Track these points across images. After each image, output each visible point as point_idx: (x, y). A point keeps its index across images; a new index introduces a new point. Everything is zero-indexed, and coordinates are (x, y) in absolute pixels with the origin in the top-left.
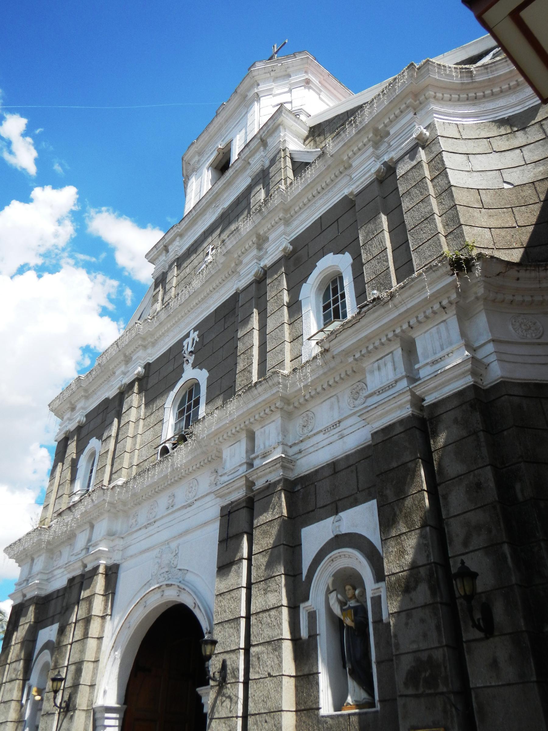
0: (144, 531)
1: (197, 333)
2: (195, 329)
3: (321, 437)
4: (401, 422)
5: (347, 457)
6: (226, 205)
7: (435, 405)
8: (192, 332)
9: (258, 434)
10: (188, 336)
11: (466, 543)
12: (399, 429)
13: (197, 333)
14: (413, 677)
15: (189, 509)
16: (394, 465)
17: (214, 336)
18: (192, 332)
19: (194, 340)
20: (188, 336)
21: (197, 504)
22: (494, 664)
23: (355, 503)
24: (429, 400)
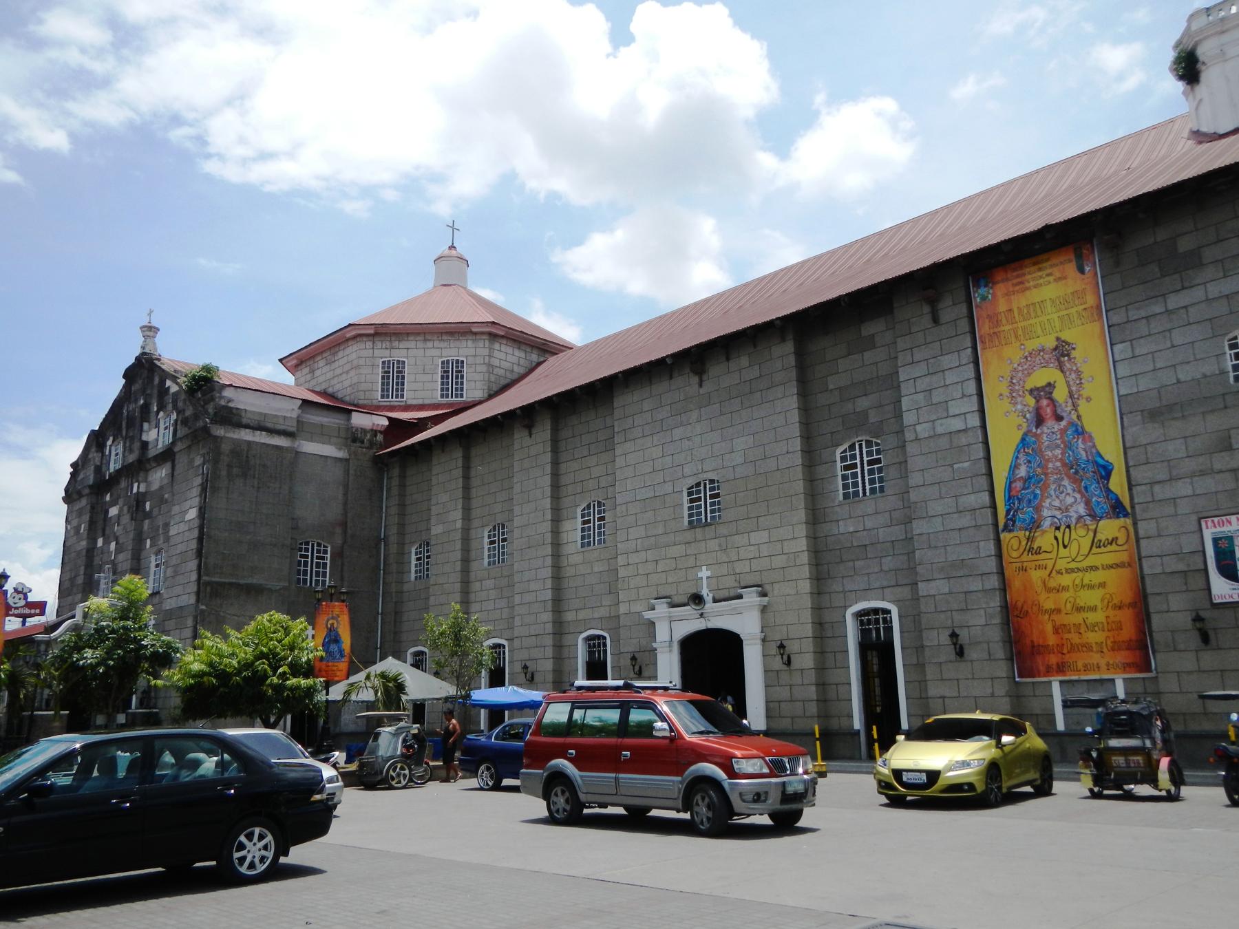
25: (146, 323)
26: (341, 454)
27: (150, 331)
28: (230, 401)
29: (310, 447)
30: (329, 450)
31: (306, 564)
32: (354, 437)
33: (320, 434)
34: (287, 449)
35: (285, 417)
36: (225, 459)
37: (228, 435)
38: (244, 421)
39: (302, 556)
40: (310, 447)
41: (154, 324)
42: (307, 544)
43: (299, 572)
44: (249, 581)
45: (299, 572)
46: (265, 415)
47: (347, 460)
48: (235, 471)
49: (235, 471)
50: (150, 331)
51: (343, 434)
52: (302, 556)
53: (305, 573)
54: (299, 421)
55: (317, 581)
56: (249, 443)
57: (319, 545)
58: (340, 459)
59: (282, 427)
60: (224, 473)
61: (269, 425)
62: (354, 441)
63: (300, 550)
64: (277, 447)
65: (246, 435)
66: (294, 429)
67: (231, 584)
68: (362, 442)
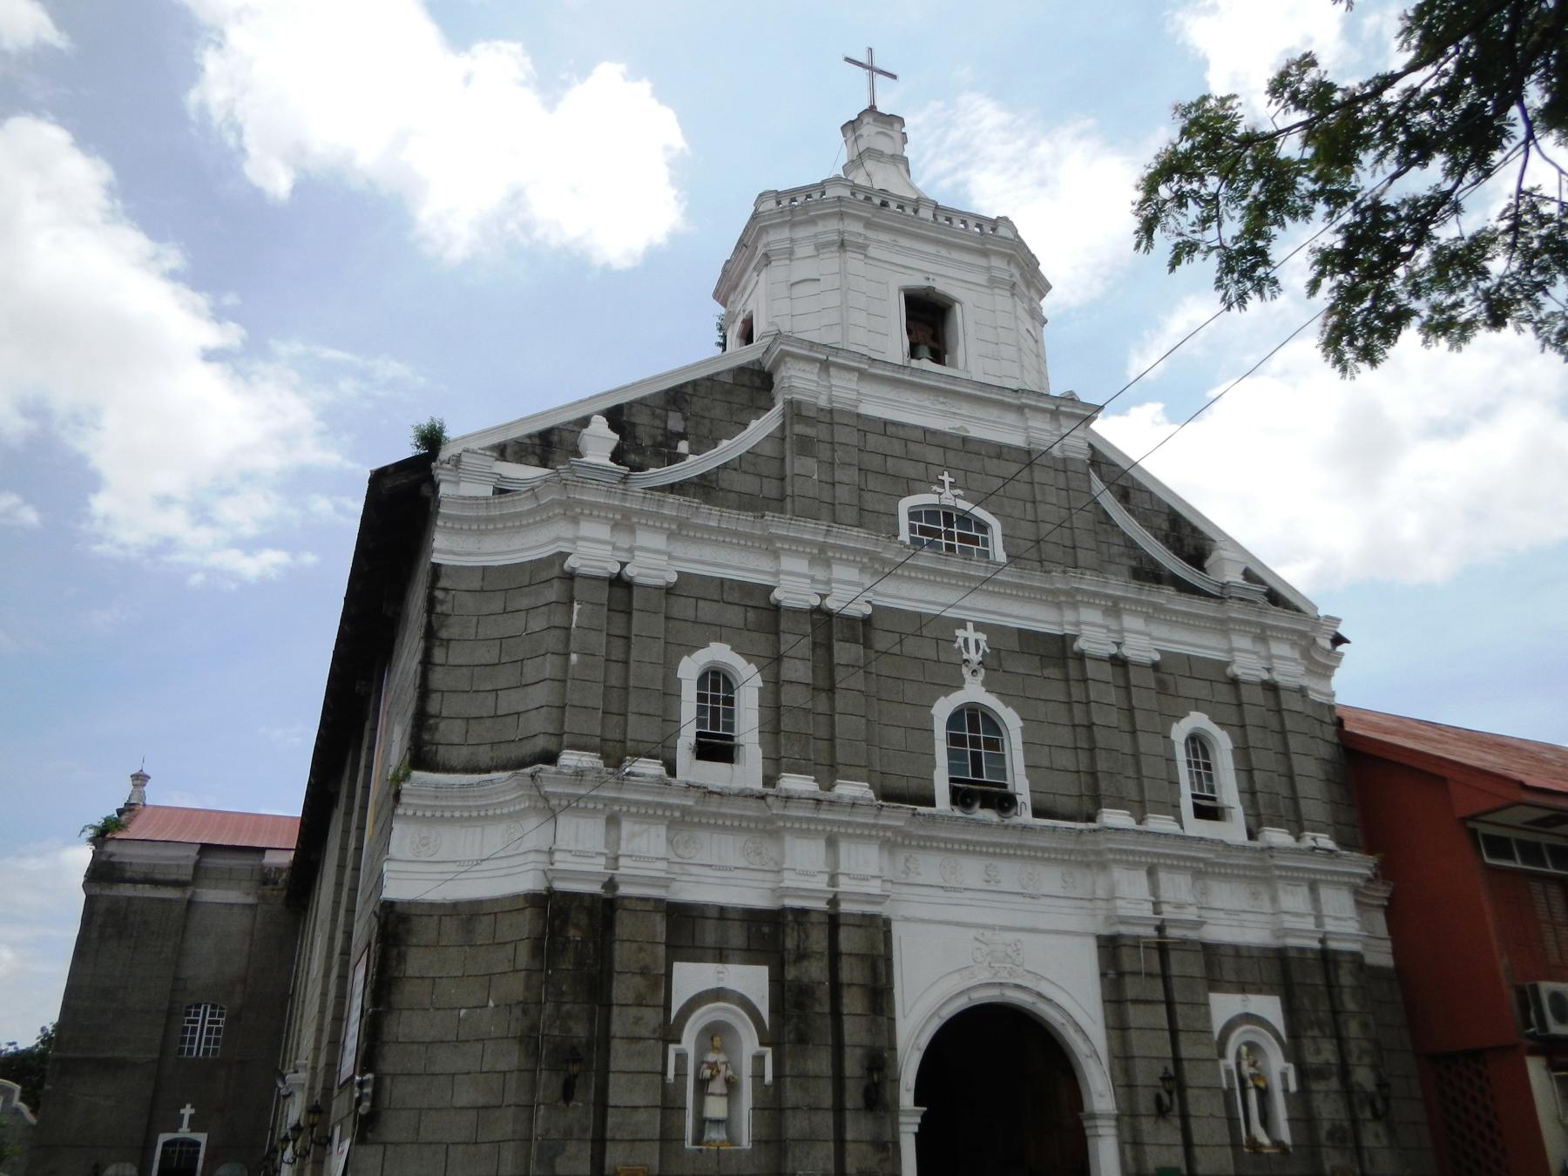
0: (941, 892)
1: (984, 637)
2: (979, 627)
3: (1221, 915)
4: (1312, 950)
5: (1249, 948)
6: (976, 432)
7: (1336, 952)
8: (970, 626)
9: (1163, 876)
10: (962, 624)
11: (1360, 1058)
12: (1310, 955)
13: (984, 637)
14: (1331, 1135)
15: (1028, 900)
16: (1308, 981)
17: (1022, 671)
18: (970, 626)
19: (977, 642)
20: (962, 624)
21: (1043, 900)
22: (1377, 1136)
23: (1260, 992)
24: (1333, 945)
25: (136, 771)
26: (251, 900)
27: (140, 779)
28: (111, 855)
29: (210, 895)
30: (234, 896)
31: (194, 1030)
32: (266, 878)
33: (228, 878)
34: (176, 901)
37: (107, 892)
38: (128, 874)
40: (210, 895)
41: (146, 772)
42: (198, 1006)
44: (109, 1054)
47: (251, 906)
50: (140, 779)
53: (192, 1041)
54: (197, 867)
55: (206, 1051)
56: (129, 899)
57: (214, 1007)
58: (244, 905)
59: (173, 877)
60: (95, 935)
61: (158, 876)
63: (188, 1014)
64: (163, 900)
65: (126, 891)
66: (189, 878)
68: (276, 883)
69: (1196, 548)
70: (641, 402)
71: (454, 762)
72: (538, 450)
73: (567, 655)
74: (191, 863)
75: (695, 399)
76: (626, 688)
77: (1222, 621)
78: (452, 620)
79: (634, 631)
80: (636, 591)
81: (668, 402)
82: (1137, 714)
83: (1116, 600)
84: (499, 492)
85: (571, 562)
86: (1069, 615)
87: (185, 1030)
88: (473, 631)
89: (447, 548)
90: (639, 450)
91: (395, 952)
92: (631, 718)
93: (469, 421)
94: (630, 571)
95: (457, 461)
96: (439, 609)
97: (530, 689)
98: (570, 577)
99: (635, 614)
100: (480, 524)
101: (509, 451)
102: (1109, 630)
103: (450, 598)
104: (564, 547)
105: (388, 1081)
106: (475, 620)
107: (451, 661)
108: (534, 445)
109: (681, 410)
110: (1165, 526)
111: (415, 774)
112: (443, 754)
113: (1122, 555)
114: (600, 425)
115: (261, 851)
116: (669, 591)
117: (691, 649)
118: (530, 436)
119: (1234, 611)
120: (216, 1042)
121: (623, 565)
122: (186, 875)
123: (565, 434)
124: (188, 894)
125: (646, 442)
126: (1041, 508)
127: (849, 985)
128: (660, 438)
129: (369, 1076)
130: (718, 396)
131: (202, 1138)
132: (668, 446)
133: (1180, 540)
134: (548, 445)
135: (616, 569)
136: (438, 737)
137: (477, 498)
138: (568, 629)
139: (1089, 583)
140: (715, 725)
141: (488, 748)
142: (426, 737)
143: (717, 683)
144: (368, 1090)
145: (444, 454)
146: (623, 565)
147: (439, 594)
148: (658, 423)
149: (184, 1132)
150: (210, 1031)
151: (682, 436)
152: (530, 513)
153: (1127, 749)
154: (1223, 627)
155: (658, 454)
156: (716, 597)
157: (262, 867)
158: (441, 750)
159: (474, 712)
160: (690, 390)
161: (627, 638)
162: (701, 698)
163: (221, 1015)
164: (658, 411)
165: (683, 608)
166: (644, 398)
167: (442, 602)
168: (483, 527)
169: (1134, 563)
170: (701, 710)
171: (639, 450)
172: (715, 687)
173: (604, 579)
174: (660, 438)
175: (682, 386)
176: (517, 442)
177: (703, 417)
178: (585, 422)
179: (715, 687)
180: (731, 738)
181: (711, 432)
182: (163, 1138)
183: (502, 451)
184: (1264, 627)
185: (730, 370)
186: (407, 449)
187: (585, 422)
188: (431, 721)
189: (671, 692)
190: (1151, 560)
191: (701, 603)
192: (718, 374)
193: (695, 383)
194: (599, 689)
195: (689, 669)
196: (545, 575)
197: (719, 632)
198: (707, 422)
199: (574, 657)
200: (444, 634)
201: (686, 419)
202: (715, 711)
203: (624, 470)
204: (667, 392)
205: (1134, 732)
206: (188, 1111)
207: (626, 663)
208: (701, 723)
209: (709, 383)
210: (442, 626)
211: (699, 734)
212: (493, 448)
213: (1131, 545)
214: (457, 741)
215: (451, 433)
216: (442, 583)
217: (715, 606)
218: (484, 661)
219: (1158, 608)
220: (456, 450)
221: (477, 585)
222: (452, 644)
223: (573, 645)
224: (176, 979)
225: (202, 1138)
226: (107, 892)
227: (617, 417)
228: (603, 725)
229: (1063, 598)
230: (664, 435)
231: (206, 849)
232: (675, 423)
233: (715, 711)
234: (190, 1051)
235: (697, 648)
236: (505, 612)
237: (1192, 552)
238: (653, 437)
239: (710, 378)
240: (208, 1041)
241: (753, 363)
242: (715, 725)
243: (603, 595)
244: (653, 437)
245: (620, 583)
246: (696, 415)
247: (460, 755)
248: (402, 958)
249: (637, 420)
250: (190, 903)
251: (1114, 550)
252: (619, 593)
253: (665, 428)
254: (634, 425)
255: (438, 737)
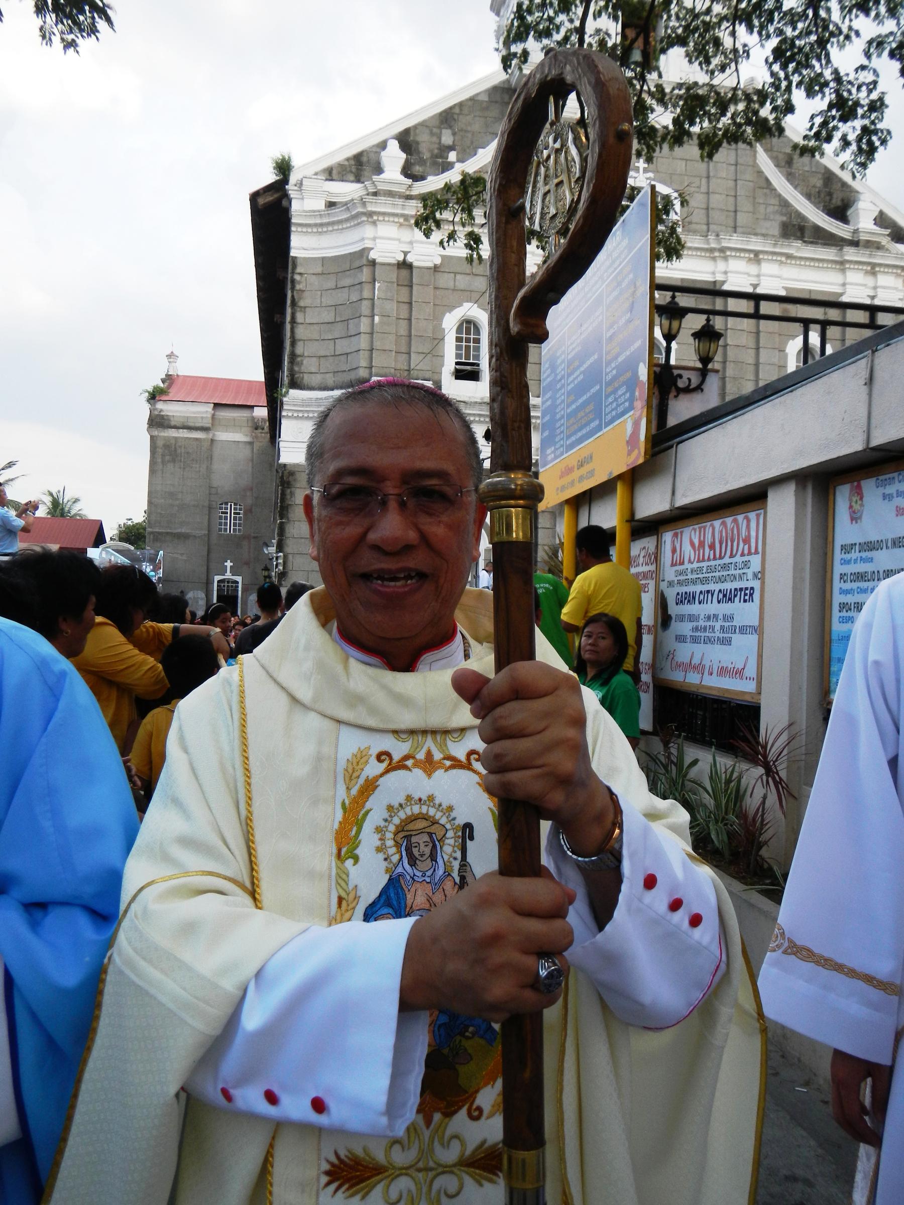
25: (169, 353)
29: (223, 436)
30: (239, 436)
31: (226, 518)
33: (233, 425)
34: (204, 439)
35: (202, 418)
36: (160, 451)
37: (162, 434)
38: (173, 423)
39: (222, 513)
40: (223, 436)
42: (226, 504)
43: (220, 524)
44: (179, 531)
45: (220, 524)
46: (188, 417)
48: (167, 458)
49: (167, 458)
51: (250, 424)
52: (222, 513)
53: (226, 524)
56: (176, 438)
60: (159, 460)
61: (191, 424)
62: (256, 429)
63: (221, 508)
64: (197, 439)
65: (173, 433)
66: (209, 425)
67: (167, 533)
68: (263, 429)
69: (843, 200)
70: (423, 124)
71: (314, 384)
72: (354, 170)
73: (373, 316)
74: (209, 416)
75: (461, 117)
76: (410, 336)
77: (842, 263)
78: (306, 294)
79: (414, 299)
80: (414, 271)
81: (442, 122)
82: (762, 335)
83: (757, 253)
84: (331, 205)
85: (373, 255)
86: (721, 266)
87: (221, 518)
88: (319, 301)
89: (301, 245)
90: (422, 162)
91: (288, 491)
92: (413, 355)
93: (314, 147)
94: (410, 258)
95: (300, 184)
96: (298, 287)
97: (352, 338)
98: (373, 263)
99: (415, 287)
100: (320, 228)
101: (334, 172)
102: (748, 274)
103: (303, 279)
104: (368, 244)
105: (290, 557)
106: (319, 293)
107: (308, 321)
108: (350, 166)
109: (450, 127)
110: (819, 183)
111: (292, 391)
112: (307, 379)
113: (775, 213)
114: (394, 145)
115: (252, 407)
116: (436, 268)
117: (451, 308)
118: (348, 159)
119: (850, 254)
120: (240, 525)
121: (405, 254)
122: (207, 423)
123: (372, 156)
124: (210, 436)
125: (426, 155)
126: (713, 181)
127: (543, 512)
128: (436, 151)
129: (281, 554)
130: (477, 113)
131: (239, 579)
132: (441, 157)
133: (830, 194)
134: (361, 166)
135: (401, 258)
136: (303, 369)
137: (314, 211)
138: (373, 299)
139: (734, 241)
140: (467, 356)
141: (331, 375)
142: (296, 369)
143: (468, 326)
144: (280, 561)
145: (293, 178)
146: (405, 254)
147: (297, 277)
148: (435, 139)
149: (228, 575)
150: (235, 519)
151: (451, 148)
152: (347, 220)
153: (751, 360)
154: (842, 265)
155: (434, 164)
156: (468, 271)
157: (253, 418)
158: (306, 376)
159: (322, 353)
160: (457, 110)
161: (410, 303)
162: (459, 339)
163: (240, 509)
164: (435, 130)
165: (445, 280)
166: (424, 121)
167: (299, 283)
168: (320, 230)
169: (784, 219)
170: (458, 348)
171: (422, 162)
172: (468, 332)
173: (393, 265)
174: (436, 151)
175: (451, 108)
176: (340, 165)
177: (466, 131)
178: (383, 145)
179: (468, 332)
180: (478, 365)
181: (472, 143)
182: (217, 578)
183: (330, 174)
184: (873, 265)
185: (486, 91)
186: (269, 177)
187: (383, 145)
188: (299, 359)
189: (438, 339)
190: (799, 215)
191: (458, 277)
192: (477, 94)
193: (461, 105)
194: (392, 338)
195: (450, 322)
196: (357, 264)
197: (468, 295)
198: (470, 135)
199: (377, 319)
200: (302, 303)
201: (454, 134)
202: (468, 348)
203: (409, 181)
204: (441, 114)
205: (758, 349)
206: (229, 564)
207: (410, 320)
208: (458, 356)
209: (470, 103)
210: (300, 299)
211: (457, 363)
212: (324, 171)
213: (785, 204)
214: (313, 370)
215: (295, 163)
216: (299, 270)
217: (468, 278)
218: (326, 321)
219: (789, 256)
220: (300, 177)
221: (319, 270)
222: (307, 309)
223: (376, 311)
224: (210, 487)
225: (239, 579)
226: (162, 434)
227: (406, 140)
228: (396, 361)
229: (717, 254)
230: (440, 149)
231: (217, 405)
232: (447, 138)
233: (468, 348)
234: (226, 530)
235: (454, 307)
236: (337, 288)
237: (839, 203)
238: (431, 151)
239: (472, 99)
240: (235, 525)
241: (504, 82)
242: (467, 356)
243: (393, 275)
244: (431, 151)
245: (405, 265)
246: (462, 130)
247: (316, 380)
248: (292, 494)
249: (419, 139)
250: (212, 440)
251: (770, 209)
252: (404, 273)
253: (440, 143)
254: (417, 143)
255: (303, 369)
